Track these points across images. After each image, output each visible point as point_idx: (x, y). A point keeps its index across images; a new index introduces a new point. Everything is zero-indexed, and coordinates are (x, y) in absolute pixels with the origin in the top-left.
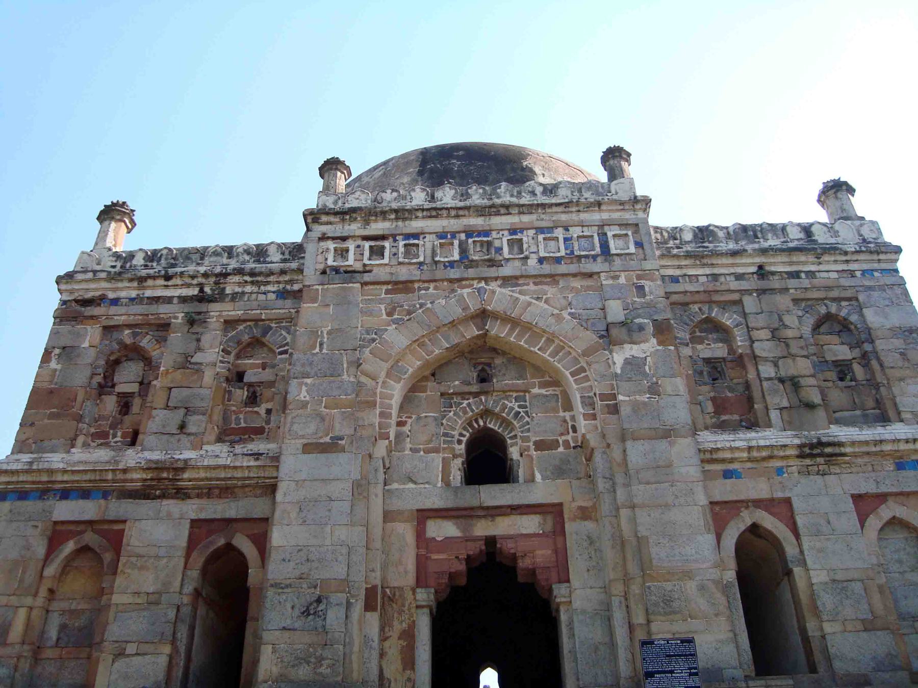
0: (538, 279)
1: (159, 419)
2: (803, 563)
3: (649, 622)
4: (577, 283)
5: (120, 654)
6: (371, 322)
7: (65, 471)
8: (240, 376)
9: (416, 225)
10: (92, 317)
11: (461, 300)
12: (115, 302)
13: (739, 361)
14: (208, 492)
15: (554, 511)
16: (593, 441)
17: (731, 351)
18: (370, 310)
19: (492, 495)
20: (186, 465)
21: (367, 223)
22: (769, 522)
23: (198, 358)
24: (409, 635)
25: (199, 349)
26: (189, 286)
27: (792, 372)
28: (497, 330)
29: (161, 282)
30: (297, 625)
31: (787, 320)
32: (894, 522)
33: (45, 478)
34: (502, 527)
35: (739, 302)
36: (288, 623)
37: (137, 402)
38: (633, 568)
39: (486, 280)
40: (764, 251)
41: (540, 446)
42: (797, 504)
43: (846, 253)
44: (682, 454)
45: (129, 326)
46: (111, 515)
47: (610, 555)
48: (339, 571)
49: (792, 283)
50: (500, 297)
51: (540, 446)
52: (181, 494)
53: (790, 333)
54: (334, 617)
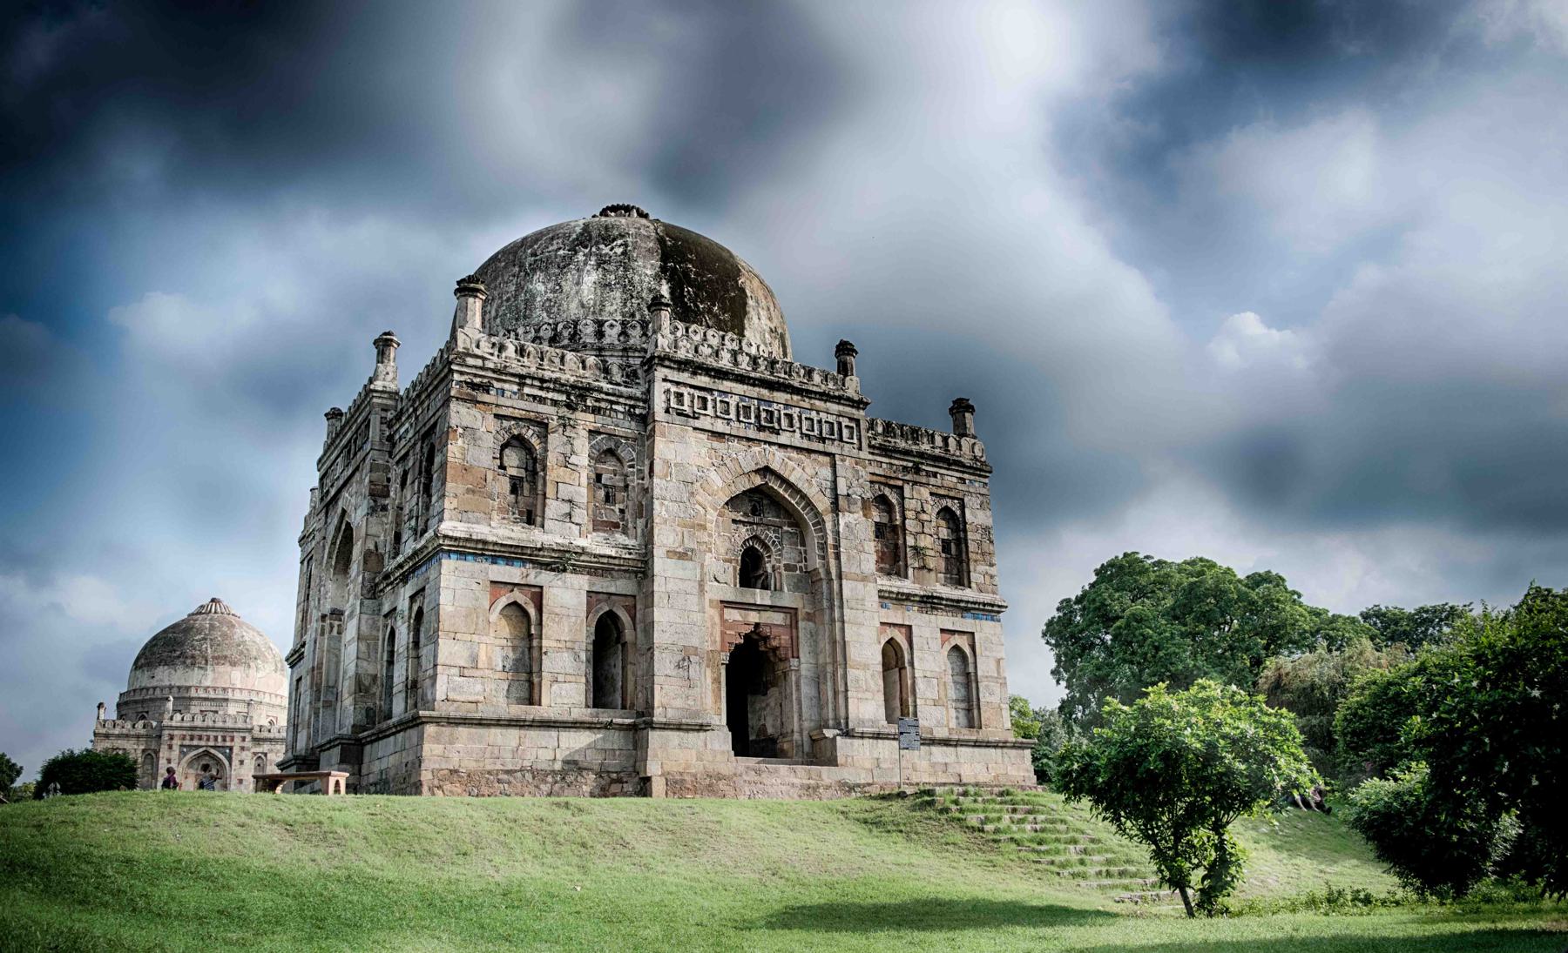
0: (799, 449)
1: (554, 508)
2: (912, 664)
4: (821, 458)
7: (496, 544)
8: (599, 477)
9: (727, 385)
13: (894, 529)
14: (592, 571)
15: (792, 612)
17: (891, 520)
19: (760, 596)
20: (584, 551)
21: (694, 373)
22: (901, 639)
23: (573, 459)
25: (573, 452)
26: (559, 391)
27: (922, 545)
29: (537, 383)
31: (928, 508)
32: (956, 648)
35: (901, 489)
36: (668, 672)
37: (526, 486)
39: (771, 444)
40: (921, 455)
41: (788, 568)
42: (914, 629)
43: (963, 465)
44: (870, 593)
45: (514, 418)
46: (532, 580)
49: (932, 481)
51: (788, 568)
52: (576, 570)
53: (924, 517)
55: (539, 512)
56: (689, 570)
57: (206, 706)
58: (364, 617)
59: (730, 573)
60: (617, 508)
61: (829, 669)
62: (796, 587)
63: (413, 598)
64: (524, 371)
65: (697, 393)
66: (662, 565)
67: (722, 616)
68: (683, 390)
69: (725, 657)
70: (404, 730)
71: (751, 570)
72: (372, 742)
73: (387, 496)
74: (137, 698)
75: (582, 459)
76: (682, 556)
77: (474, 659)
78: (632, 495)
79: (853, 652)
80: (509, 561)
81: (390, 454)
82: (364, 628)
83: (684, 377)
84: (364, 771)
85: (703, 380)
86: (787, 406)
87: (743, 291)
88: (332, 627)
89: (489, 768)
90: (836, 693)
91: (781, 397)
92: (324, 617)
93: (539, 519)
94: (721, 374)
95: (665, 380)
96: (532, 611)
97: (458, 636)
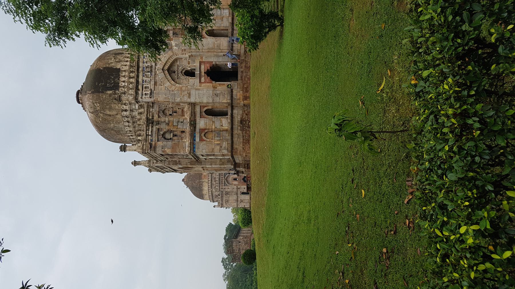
5: (222, 125)
6: (163, 89)
8: (170, 115)
9: (140, 80)
11: (160, 73)
12: (152, 140)
15: (200, 63)
16: (190, 54)
18: (161, 88)
19: (197, 72)
20: (190, 119)
21: (138, 90)
24: (220, 84)
25: (165, 122)
28: (166, 67)
34: (203, 71)
37: (175, 133)
38: (213, 50)
41: (189, 64)
47: (210, 54)
48: (211, 92)
50: (160, 66)
51: (189, 64)
52: (195, 121)
54: (218, 92)
56: (193, 92)
57: (213, 180)
59: (192, 80)
61: (215, 53)
62: (194, 61)
64: (145, 135)
65: (144, 89)
66: (192, 100)
67: (203, 83)
68: (144, 93)
69: (214, 82)
71: (190, 73)
74: (211, 198)
76: (189, 94)
77: (218, 144)
79: (211, 46)
80: (195, 137)
83: (140, 92)
85: (140, 87)
86: (144, 63)
87: (104, 68)
90: (221, 52)
91: (141, 64)
94: (137, 82)
95: (142, 98)
96: (206, 131)
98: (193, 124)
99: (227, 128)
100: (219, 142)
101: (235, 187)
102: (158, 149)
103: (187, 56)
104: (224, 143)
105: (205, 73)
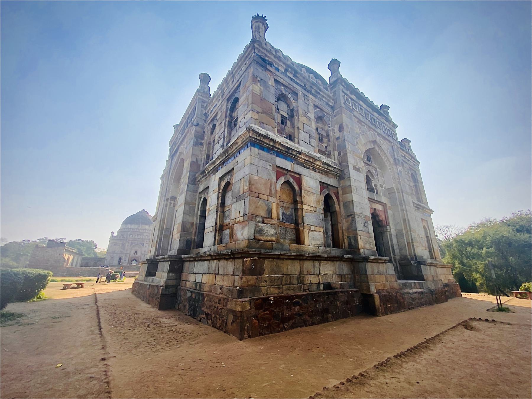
1: (303, 135)
3: (412, 242)
5: (310, 230)
7: (280, 144)
10: (270, 71)
14: (321, 172)
23: (309, 115)
28: (377, 149)
30: (364, 230)
33: (272, 144)
36: (362, 229)
37: (288, 122)
51: (381, 186)
55: (296, 136)
58: (189, 193)
60: (324, 145)
61: (404, 232)
62: (384, 195)
63: (221, 179)
70: (219, 260)
72: (190, 261)
73: (203, 138)
75: (312, 116)
77: (269, 212)
78: (331, 140)
81: (205, 121)
82: (188, 199)
84: (184, 277)
85: (354, 97)
88: (171, 203)
89: (285, 293)
92: (167, 200)
93: (296, 140)
96: (297, 188)
97: (261, 196)
98: (309, 163)
99: (306, 241)
100: (274, 215)
101: (128, 252)
102: (260, 69)
103: (394, 186)
104: (272, 231)
105: (375, 209)
